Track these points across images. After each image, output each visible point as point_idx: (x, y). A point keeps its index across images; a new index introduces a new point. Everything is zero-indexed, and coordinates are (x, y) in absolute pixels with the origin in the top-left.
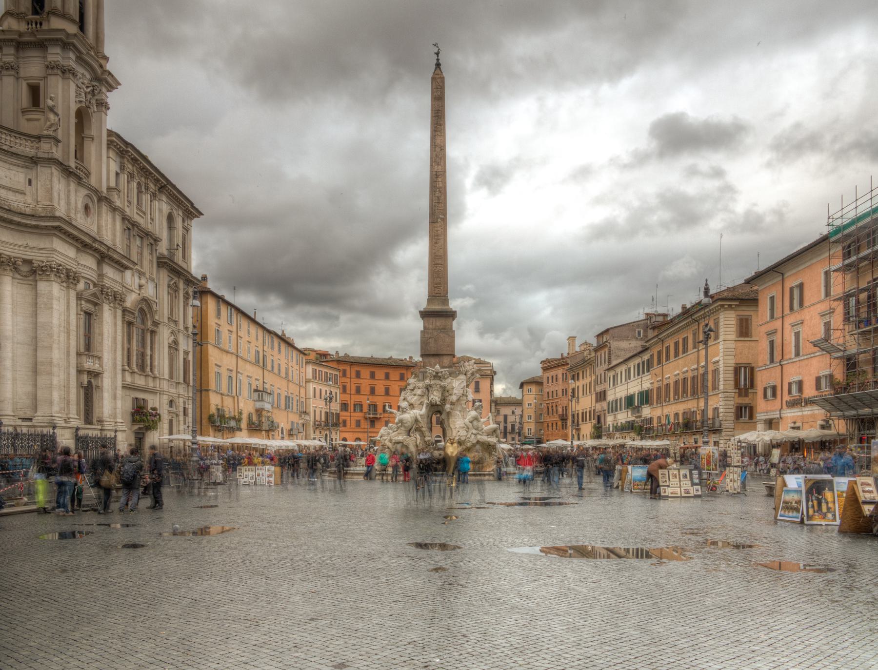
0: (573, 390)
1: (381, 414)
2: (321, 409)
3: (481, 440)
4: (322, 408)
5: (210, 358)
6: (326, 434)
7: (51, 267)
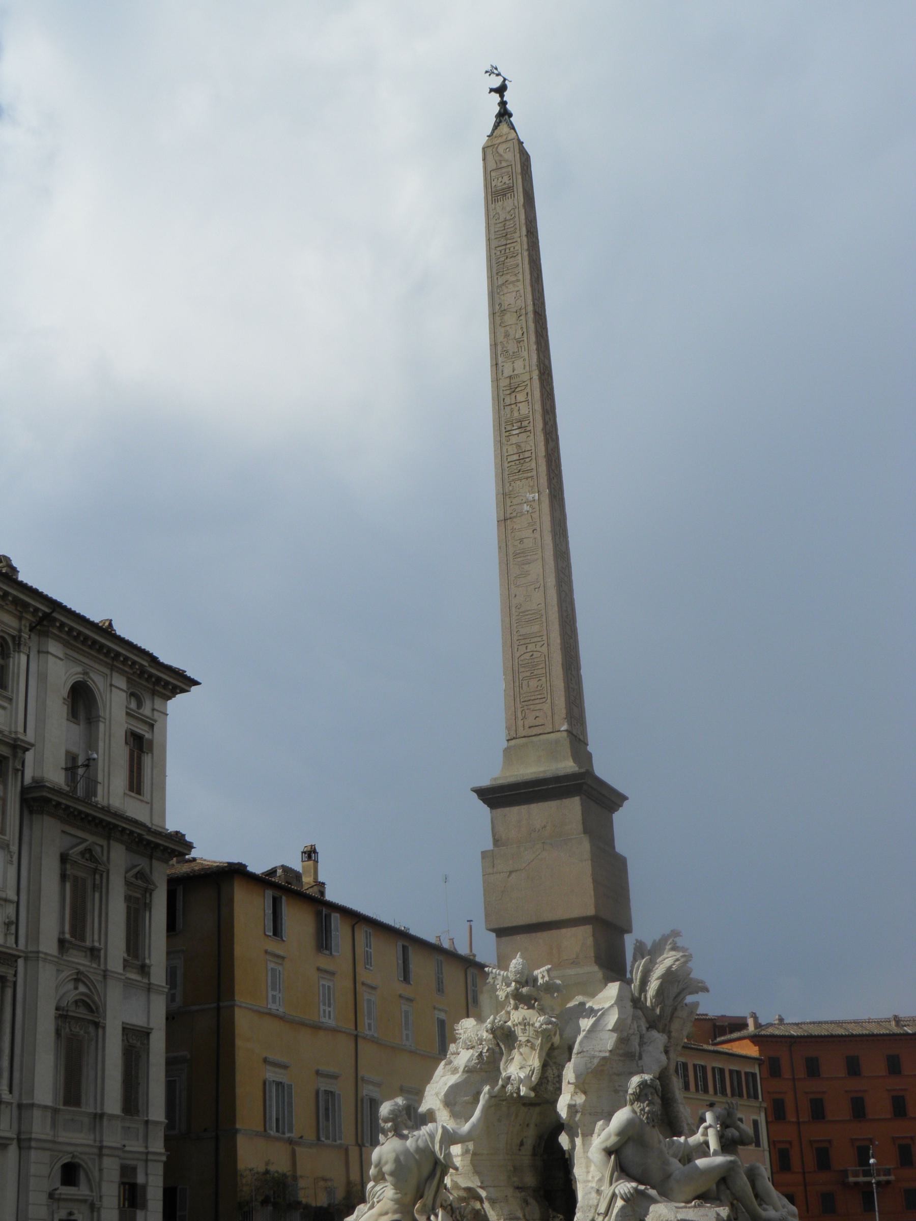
5: (239, 1042)
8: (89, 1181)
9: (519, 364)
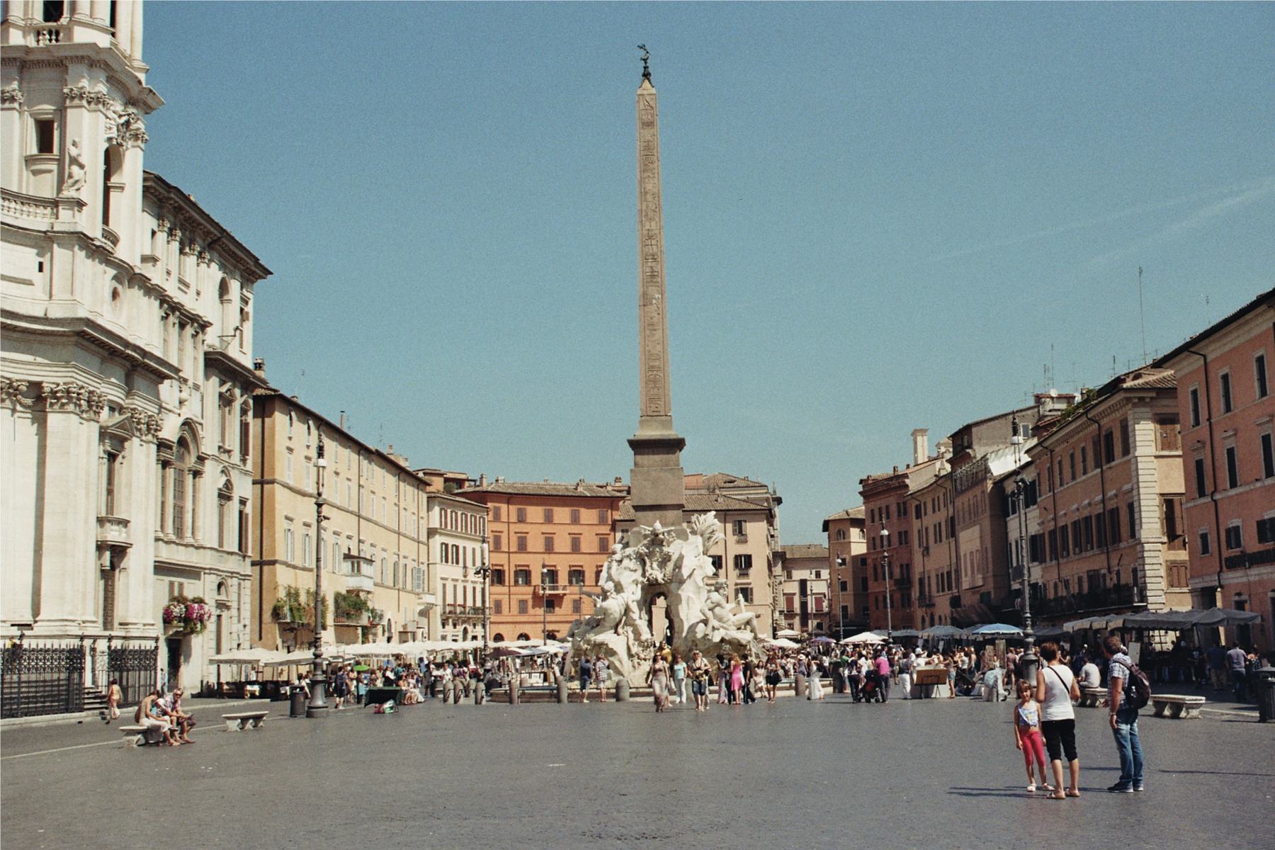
1: (565, 587)
3: (727, 638)
4: (457, 580)
5: (277, 505)
6: (465, 630)
8: (226, 591)
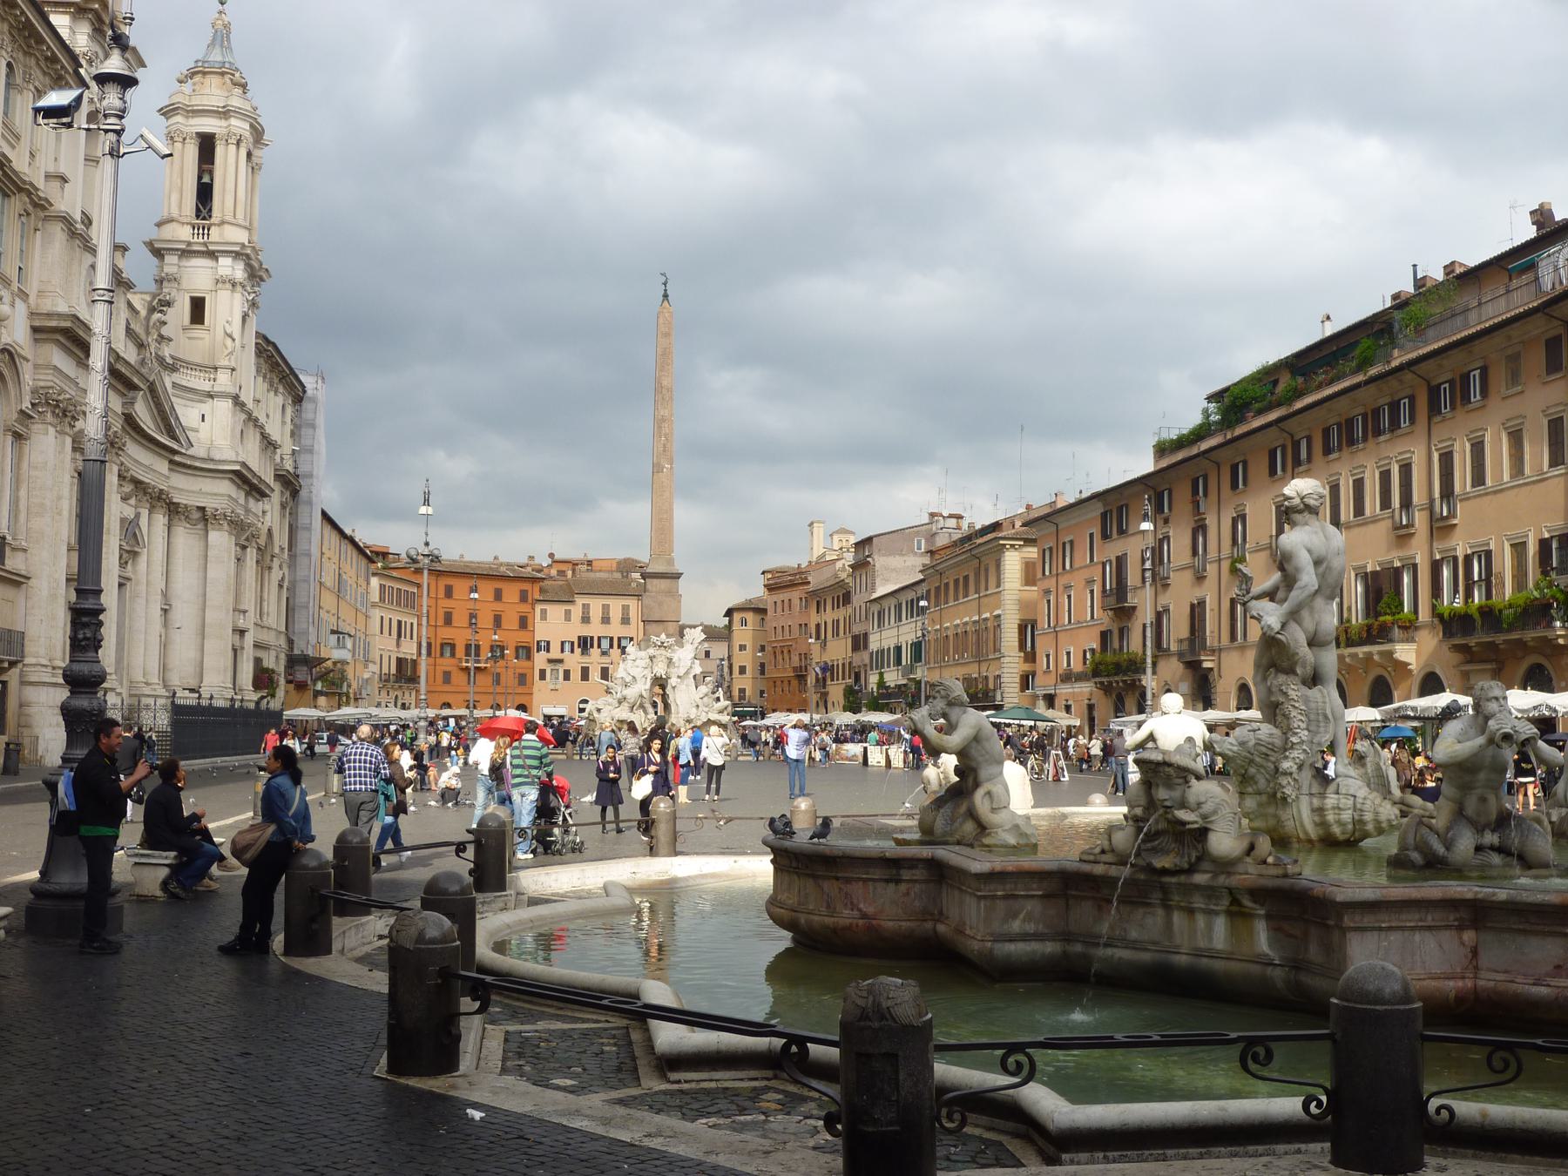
0: (818, 626)
2: (382, 652)
6: (396, 697)
7: (225, 516)
9: (666, 411)
